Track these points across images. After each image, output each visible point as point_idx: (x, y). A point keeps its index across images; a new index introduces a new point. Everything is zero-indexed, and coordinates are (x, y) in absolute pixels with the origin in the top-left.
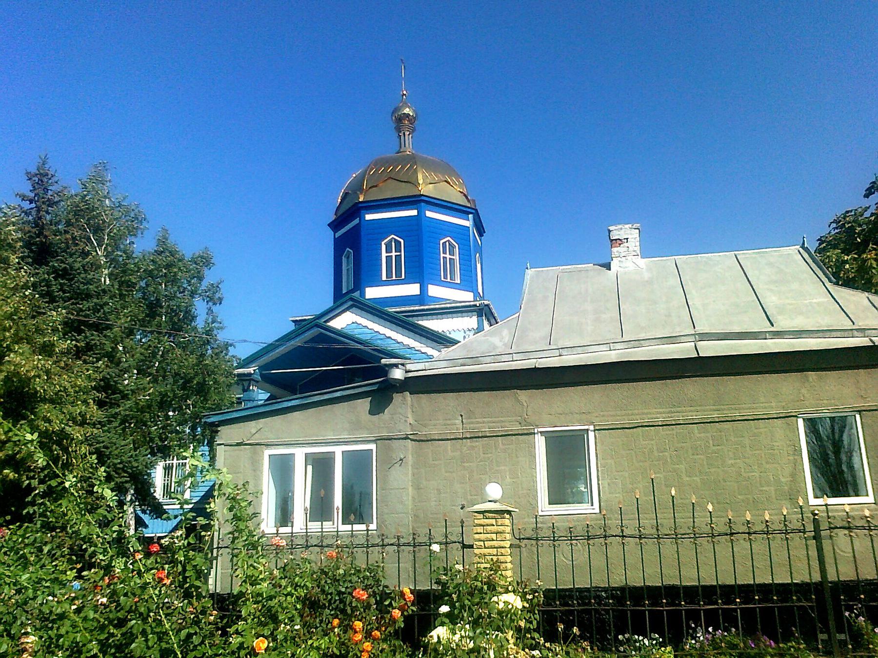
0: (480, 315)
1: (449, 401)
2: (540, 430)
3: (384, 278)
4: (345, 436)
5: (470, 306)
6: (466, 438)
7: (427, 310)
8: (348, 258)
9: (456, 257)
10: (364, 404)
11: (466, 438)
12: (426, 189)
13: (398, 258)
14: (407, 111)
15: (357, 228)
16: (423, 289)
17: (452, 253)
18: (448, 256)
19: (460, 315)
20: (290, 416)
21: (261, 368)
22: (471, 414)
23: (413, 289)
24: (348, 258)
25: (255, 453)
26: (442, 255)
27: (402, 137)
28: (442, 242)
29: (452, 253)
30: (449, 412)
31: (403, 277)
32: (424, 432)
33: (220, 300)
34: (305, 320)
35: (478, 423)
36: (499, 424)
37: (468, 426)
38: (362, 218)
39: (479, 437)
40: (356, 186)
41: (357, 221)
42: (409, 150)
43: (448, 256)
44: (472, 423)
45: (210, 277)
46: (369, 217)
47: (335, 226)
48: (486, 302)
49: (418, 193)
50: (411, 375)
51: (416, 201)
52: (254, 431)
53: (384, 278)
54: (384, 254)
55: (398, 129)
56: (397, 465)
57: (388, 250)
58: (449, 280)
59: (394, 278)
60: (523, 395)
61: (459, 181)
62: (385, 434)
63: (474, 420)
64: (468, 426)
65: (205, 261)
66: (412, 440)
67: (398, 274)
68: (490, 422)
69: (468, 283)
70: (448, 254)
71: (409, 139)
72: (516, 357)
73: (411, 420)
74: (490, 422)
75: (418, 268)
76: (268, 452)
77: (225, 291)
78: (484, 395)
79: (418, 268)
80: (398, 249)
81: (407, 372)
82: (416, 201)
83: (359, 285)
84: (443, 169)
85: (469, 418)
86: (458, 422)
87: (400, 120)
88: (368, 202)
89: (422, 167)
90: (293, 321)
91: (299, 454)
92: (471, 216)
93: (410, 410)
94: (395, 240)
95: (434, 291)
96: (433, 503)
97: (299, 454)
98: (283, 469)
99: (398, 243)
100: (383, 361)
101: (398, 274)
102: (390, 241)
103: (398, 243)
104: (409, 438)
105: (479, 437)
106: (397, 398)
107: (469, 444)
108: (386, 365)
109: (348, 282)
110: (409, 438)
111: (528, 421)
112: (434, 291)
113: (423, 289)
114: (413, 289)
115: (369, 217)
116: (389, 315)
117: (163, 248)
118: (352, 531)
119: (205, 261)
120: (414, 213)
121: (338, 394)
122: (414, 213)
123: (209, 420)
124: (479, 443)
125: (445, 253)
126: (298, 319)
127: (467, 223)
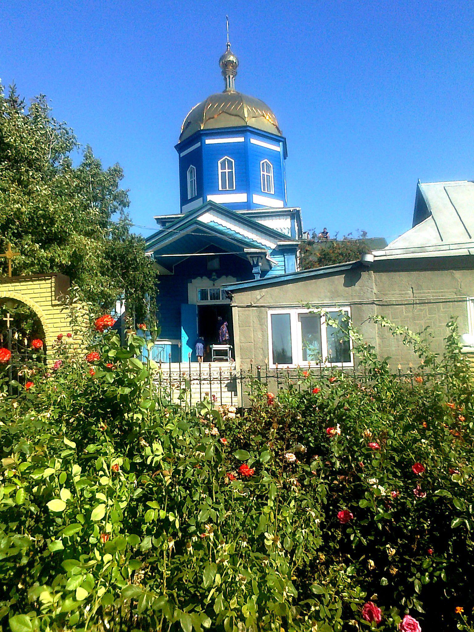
0: (292, 218)
1: (403, 278)
2: (471, 298)
3: (220, 189)
4: (326, 301)
5: (280, 212)
6: (416, 304)
7: (255, 213)
8: (191, 172)
9: (271, 174)
10: (340, 279)
11: (416, 304)
12: (251, 122)
13: (230, 174)
14: (232, 58)
15: (199, 150)
16: (249, 198)
17: (268, 171)
18: (265, 173)
19: (270, 218)
20: (285, 287)
21: (155, 253)
22: (419, 287)
23: (242, 198)
24: (191, 172)
25: (261, 312)
26: (262, 173)
27: (228, 79)
28: (261, 163)
29: (268, 171)
30: (402, 286)
31: (234, 189)
32: (386, 299)
33: (129, 203)
34: (179, 218)
35: (424, 293)
36: (441, 294)
37: (417, 295)
38: (203, 143)
39: (425, 303)
40: (197, 116)
41: (199, 144)
42: (232, 90)
43: (265, 173)
44: (420, 293)
45: (122, 186)
46: (208, 142)
47: (180, 148)
48: (298, 209)
49: (244, 124)
50: (376, 259)
51: (243, 130)
52: (259, 297)
53: (220, 189)
54: (220, 171)
55: (224, 73)
56: (367, 322)
57: (223, 167)
58: (266, 192)
59: (228, 189)
60: (458, 274)
61: (272, 116)
62: (357, 300)
63: (421, 291)
64: (417, 295)
65: (116, 173)
66: (376, 304)
67: (231, 185)
68: (434, 293)
69: (280, 193)
70: (266, 172)
71: (232, 81)
72: (452, 247)
73: (375, 291)
74: (434, 293)
75: (246, 181)
76: (270, 312)
77: (131, 197)
78: (428, 274)
79: (246, 181)
80: (230, 167)
81: (375, 256)
82: (243, 130)
83: (201, 192)
84: (260, 105)
85: (418, 290)
86: (410, 292)
87: (226, 65)
88: (208, 130)
89: (247, 104)
90: (156, 219)
91: (294, 314)
92: (281, 143)
93: (374, 284)
94: (228, 161)
95: (257, 199)
96: (394, 349)
97: (294, 314)
98: (281, 325)
99: (230, 163)
100: (246, 250)
101: (231, 185)
102: (224, 161)
103: (230, 163)
104: (374, 304)
105: (425, 303)
106: (364, 275)
107: (418, 308)
108: (248, 253)
109: (192, 191)
110: (374, 304)
111: (462, 292)
112: (257, 199)
113: (249, 198)
114: (242, 198)
115: (208, 142)
116: (235, 215)
117: (90, 164)
118: (277, 368)
119: (116, 173)
120: (241, 139)
121: (321, 272)
122: (241, 139)
123: (227, 289)
124: (426, 307)
125: (264, 171)
126: (160, 217)
127: (278, 148)
